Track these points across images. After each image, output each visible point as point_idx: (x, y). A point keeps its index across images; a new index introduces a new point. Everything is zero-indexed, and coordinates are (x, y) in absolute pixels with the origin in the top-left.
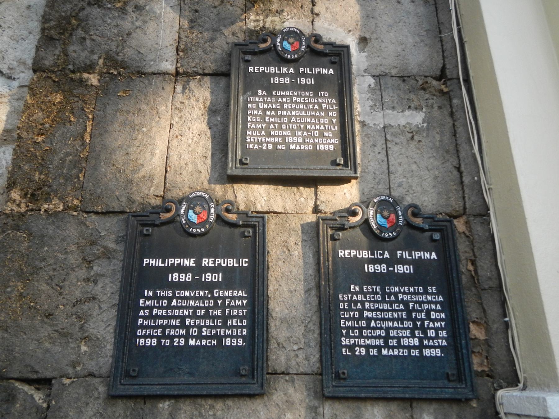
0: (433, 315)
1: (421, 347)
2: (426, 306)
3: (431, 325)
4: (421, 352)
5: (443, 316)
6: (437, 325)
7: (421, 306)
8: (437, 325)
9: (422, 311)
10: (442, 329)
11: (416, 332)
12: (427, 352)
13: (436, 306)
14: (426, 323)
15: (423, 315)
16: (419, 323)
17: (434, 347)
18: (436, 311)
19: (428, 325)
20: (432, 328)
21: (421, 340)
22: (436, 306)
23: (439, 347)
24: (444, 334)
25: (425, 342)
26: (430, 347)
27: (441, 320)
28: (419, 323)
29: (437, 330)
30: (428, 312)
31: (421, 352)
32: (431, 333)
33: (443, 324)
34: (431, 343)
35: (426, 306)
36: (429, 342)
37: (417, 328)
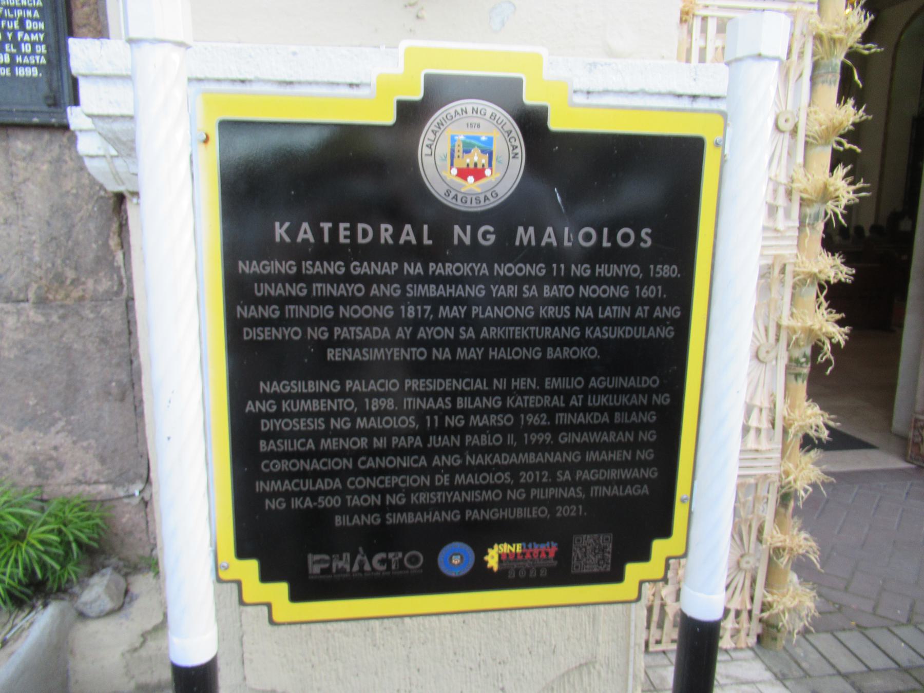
0: (29, 25)
1: (13, 65)
2: (19, 13)
3: (27, 38)
4: (13, 71)
5: (42, 26)
6: (35, 37)
7: (12, 12)
8: (35, 37)
9: (14, 19)
10: (40, 43)
11: (7, 46)
12: (20, 72)
13: (33, 13)
14: (20, 35)
15: (16, 25)
16: (10, 35)
17: (31, 66)
18: (32, 20)
19: (22, 39)
20: (26, 42)
21: (13, 57)
22: (33, 13)
23: (35, 65)
24: (42, 49)
25: (19, 59)
26: (25, 65)
27: (39, 31)
28: (10, 35)
29: (33, 44)
30: (22, 22)
31: (13, 71)
32: (26, 48)
33: (42, 36)
34: (26, 60)
35: (19, 13)
36: (23, 59)
37: (10, 42)
